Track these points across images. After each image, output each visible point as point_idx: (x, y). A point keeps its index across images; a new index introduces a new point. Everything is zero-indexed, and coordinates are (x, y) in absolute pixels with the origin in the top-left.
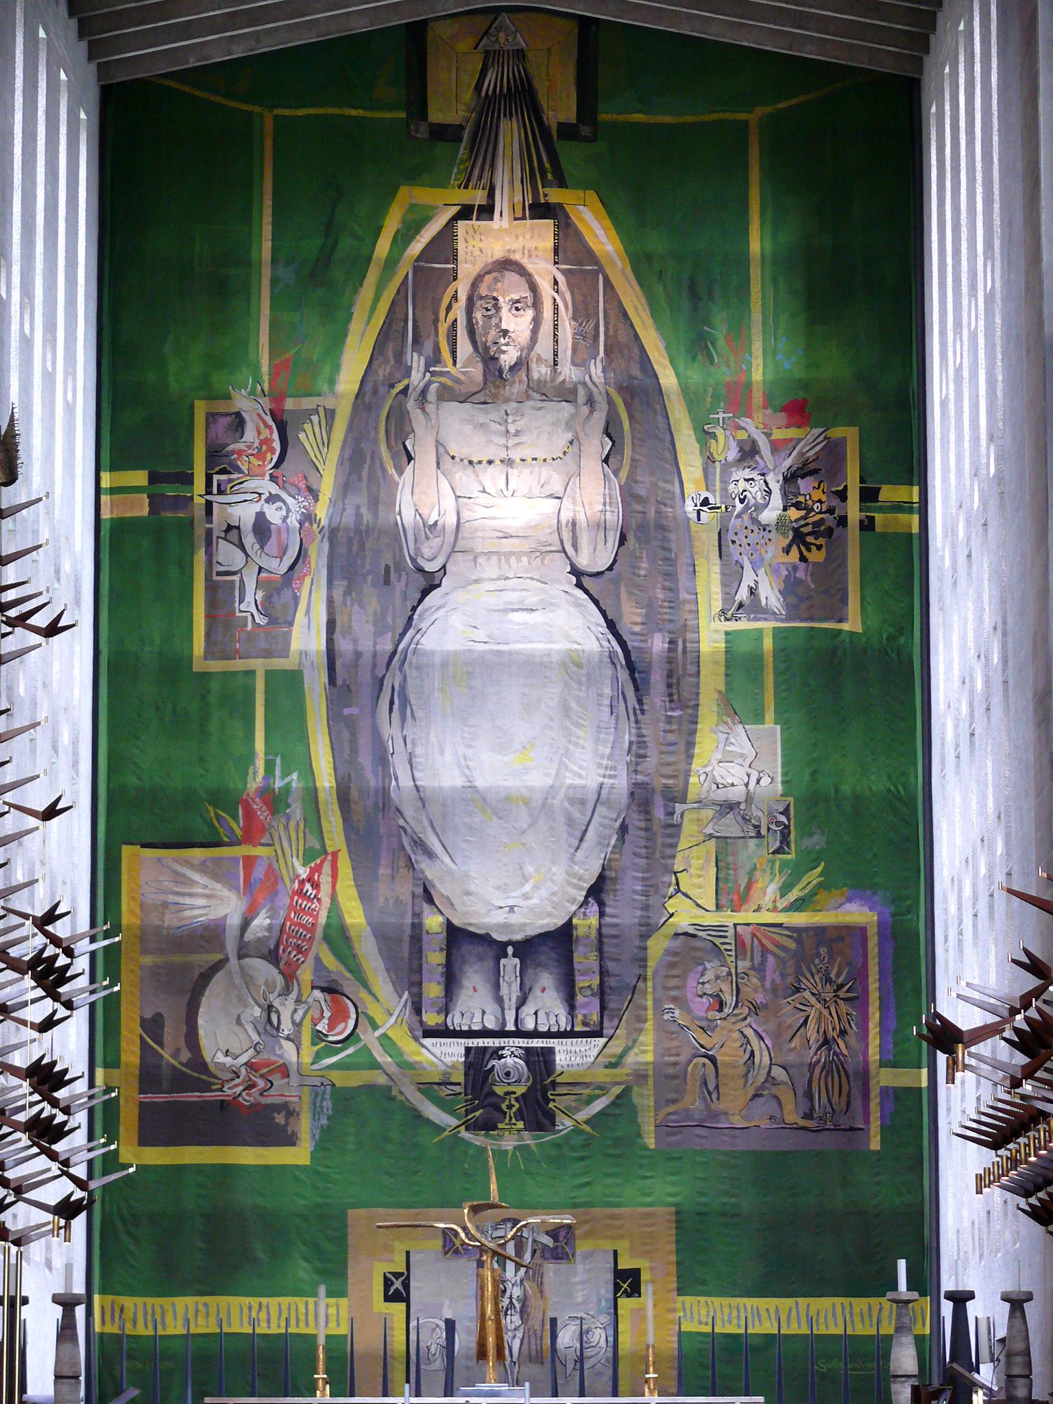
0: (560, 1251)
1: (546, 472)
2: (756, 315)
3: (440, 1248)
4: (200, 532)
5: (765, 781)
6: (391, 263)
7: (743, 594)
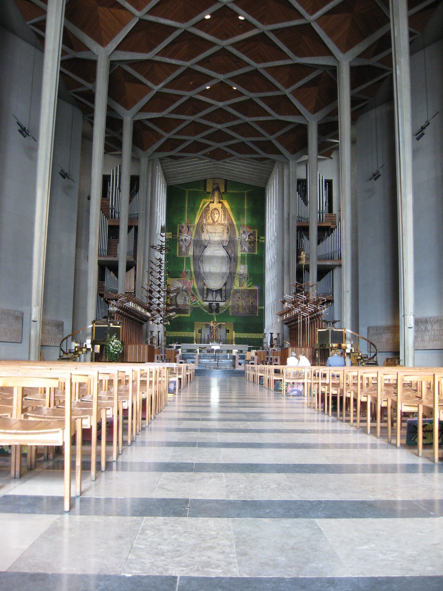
1: (220, 234)
4: (178, 240)
6: (202, 208)
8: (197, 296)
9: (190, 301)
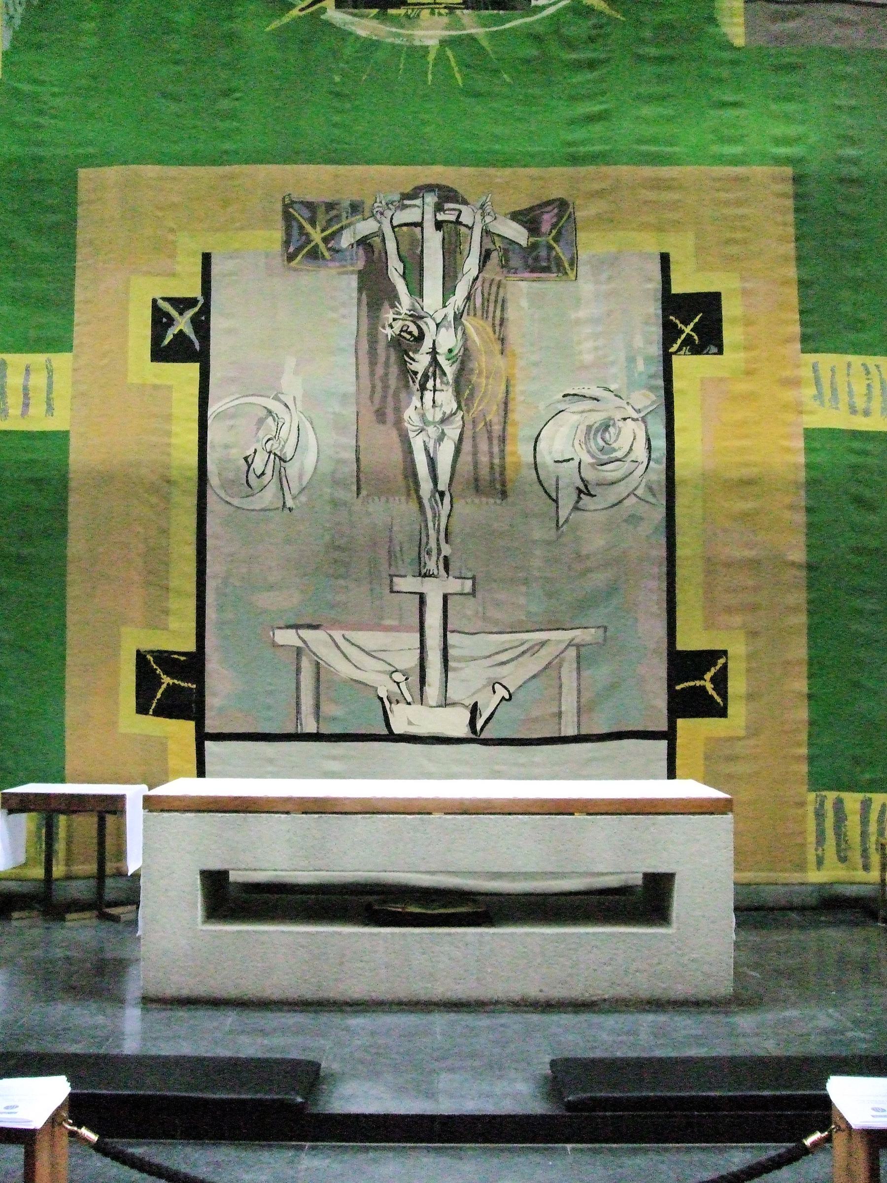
0: (543, 253)
3: (278, 247)
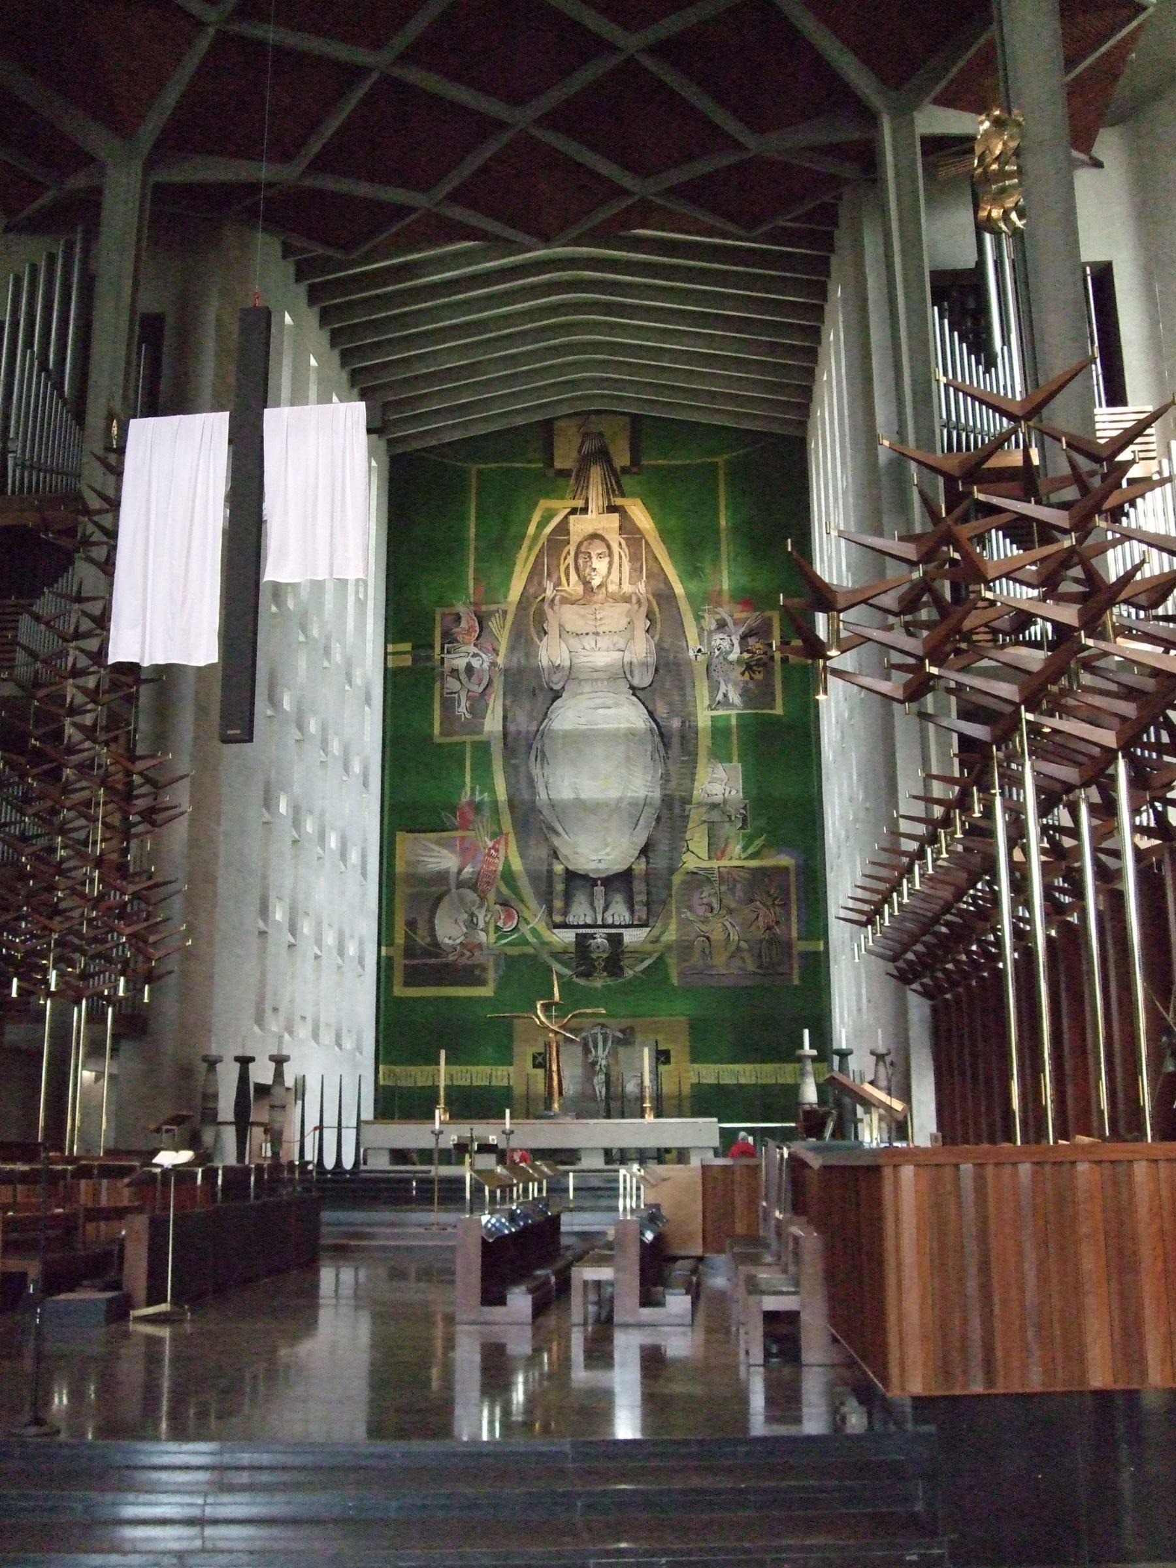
1: (616, 638)
2: (724, 556)
5: (734, 792)
7: (720, 697)
8: (521, 907)
9: (491, 929)
